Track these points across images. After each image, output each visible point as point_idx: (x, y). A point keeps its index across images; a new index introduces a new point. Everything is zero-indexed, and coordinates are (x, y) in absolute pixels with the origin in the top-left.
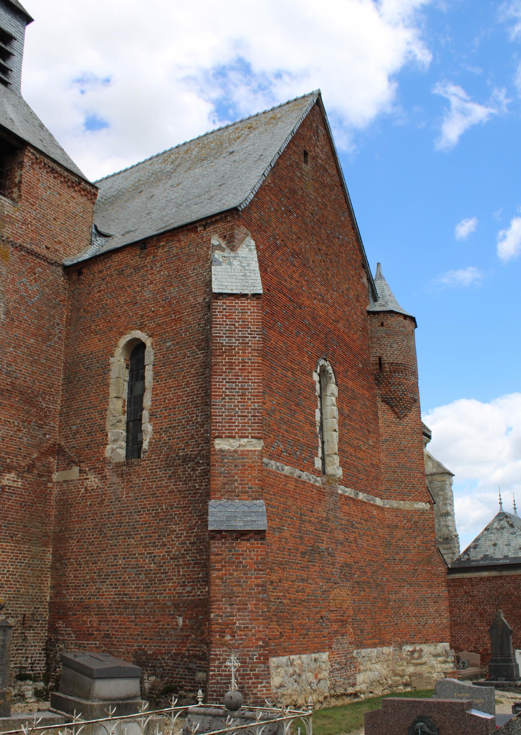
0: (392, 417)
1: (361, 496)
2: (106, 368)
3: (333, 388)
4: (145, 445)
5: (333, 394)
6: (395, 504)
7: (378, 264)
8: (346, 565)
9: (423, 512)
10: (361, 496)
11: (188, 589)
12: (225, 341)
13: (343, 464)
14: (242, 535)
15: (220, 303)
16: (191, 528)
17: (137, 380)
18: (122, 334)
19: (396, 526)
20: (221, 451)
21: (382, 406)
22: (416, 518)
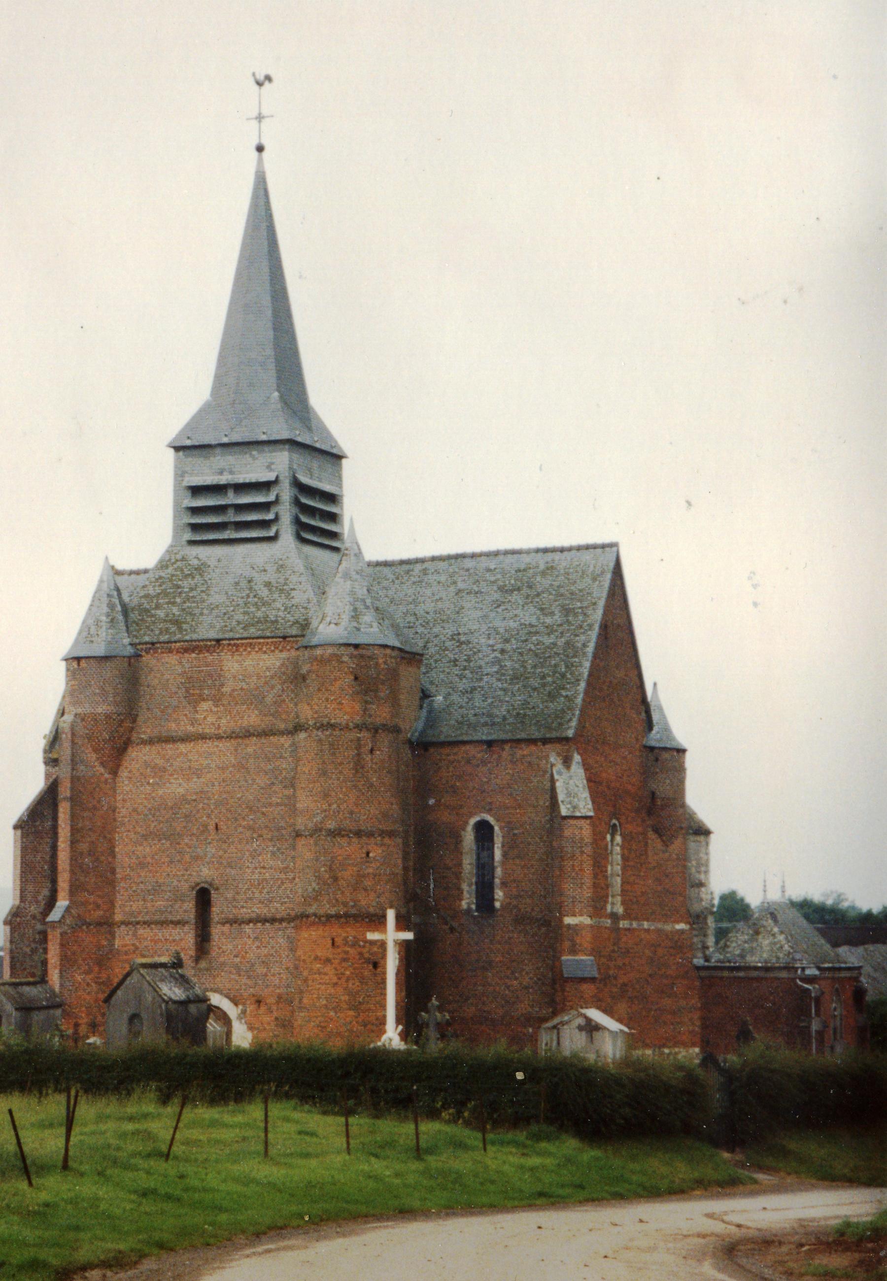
0: (659, 845)
1: (635, 925)
2: (458, 839)
3: (618, 839)
4: (497, 905)
5: (618, 844)
6: (660, 926)
7: (655, 684)
8: (625, 985)
9: (682, 932)
10: (635, 925)
11: (537, 1009)
12: (570, 850)
13: (623, 903)
14: (583, 980)
15: (566, 822)
16: (538, 968)
17: (483, 849)
18: (471, 815)
19: (660, 945)
20: (569, 925)
21: (651, 835)
22: (676, 938)
